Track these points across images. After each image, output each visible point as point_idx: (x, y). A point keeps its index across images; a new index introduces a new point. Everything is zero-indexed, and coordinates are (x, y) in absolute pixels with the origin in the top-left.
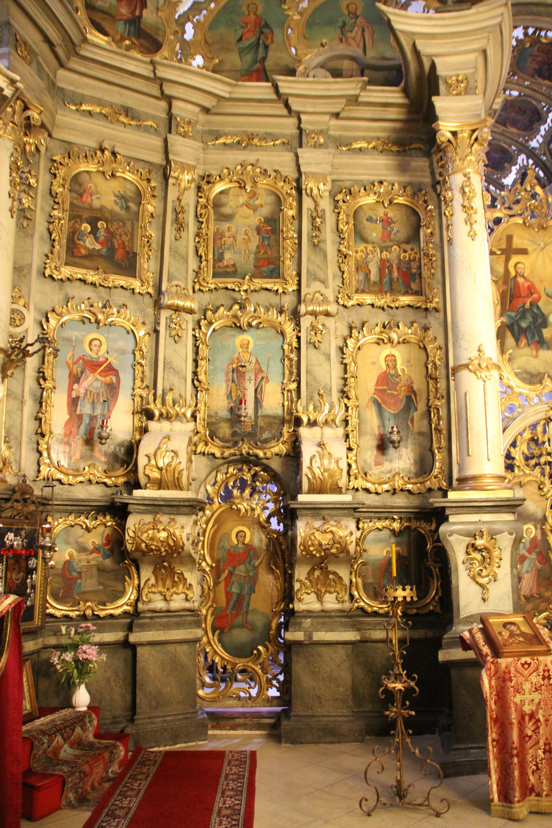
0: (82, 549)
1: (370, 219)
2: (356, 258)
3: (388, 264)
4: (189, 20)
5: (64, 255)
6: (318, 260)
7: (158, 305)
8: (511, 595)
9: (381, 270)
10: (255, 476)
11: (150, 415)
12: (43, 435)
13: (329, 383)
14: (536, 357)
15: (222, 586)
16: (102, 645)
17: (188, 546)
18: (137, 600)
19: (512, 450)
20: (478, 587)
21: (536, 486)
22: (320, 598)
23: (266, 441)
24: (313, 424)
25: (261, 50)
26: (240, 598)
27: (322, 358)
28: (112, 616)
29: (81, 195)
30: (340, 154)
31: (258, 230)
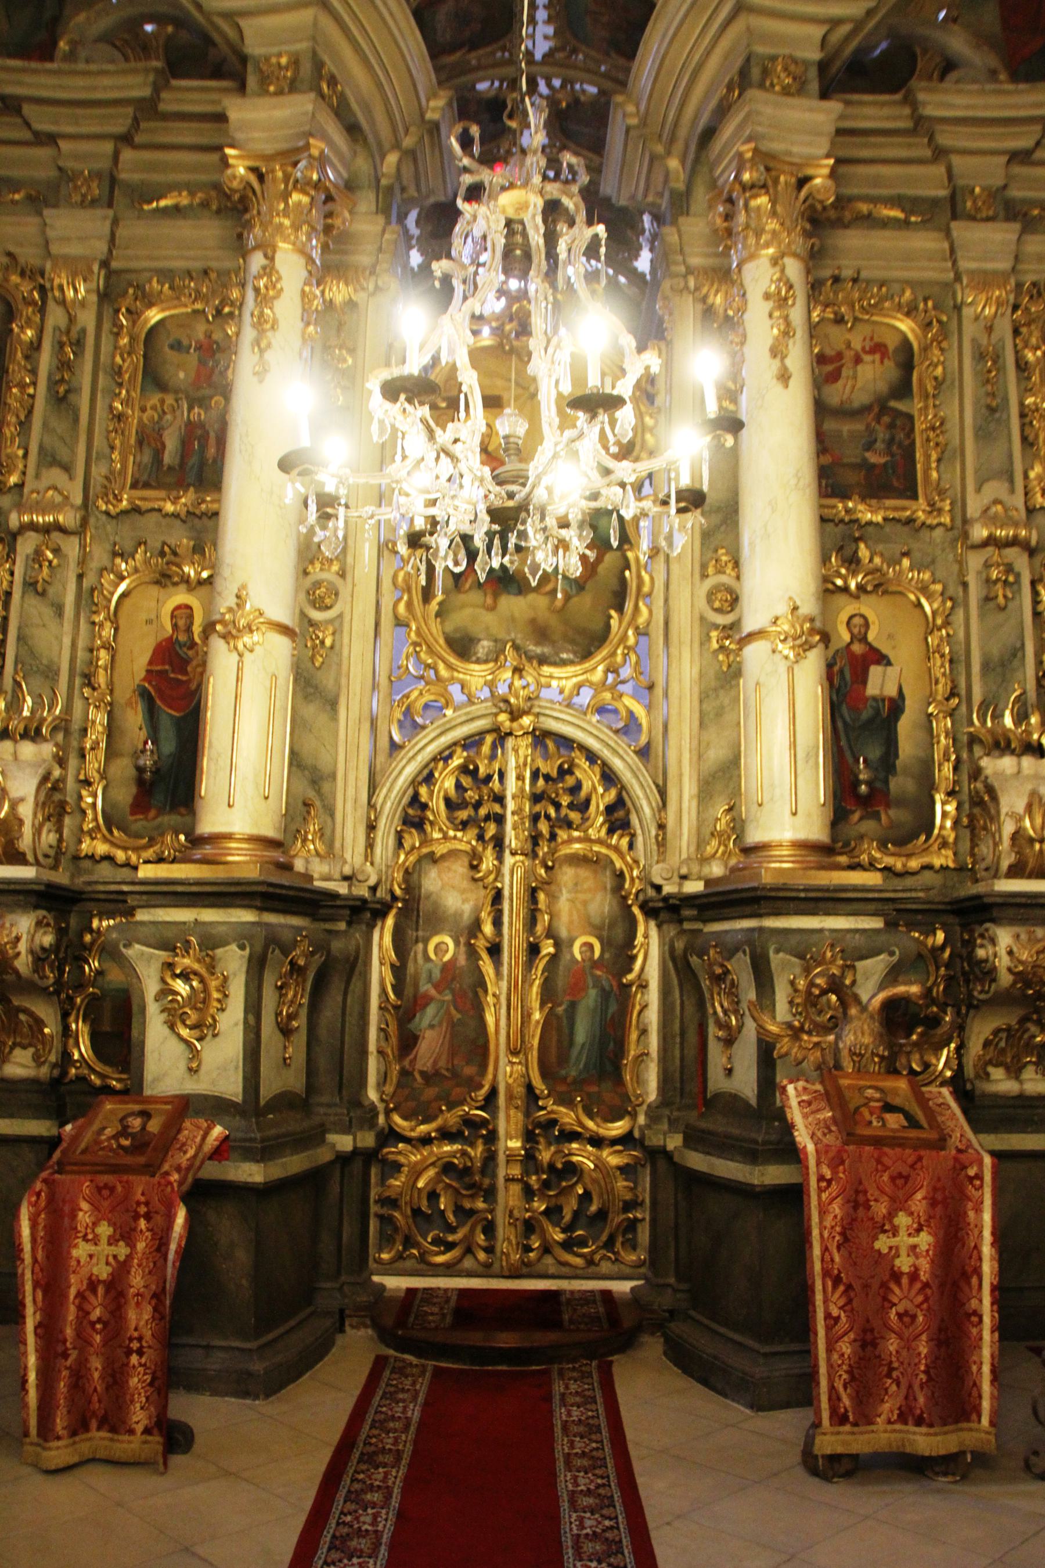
1: (177, 346)
2: (140, 420)
3: (199, 432)
6: (61, 426)
8: (241, 1064)
9: (185, 444)
13: (56, 659)
14: (492, 608)
19: (423, 790)
20: (182, 1046)
21: (466, 861)
27: (48, 612)
30: (139, 218)
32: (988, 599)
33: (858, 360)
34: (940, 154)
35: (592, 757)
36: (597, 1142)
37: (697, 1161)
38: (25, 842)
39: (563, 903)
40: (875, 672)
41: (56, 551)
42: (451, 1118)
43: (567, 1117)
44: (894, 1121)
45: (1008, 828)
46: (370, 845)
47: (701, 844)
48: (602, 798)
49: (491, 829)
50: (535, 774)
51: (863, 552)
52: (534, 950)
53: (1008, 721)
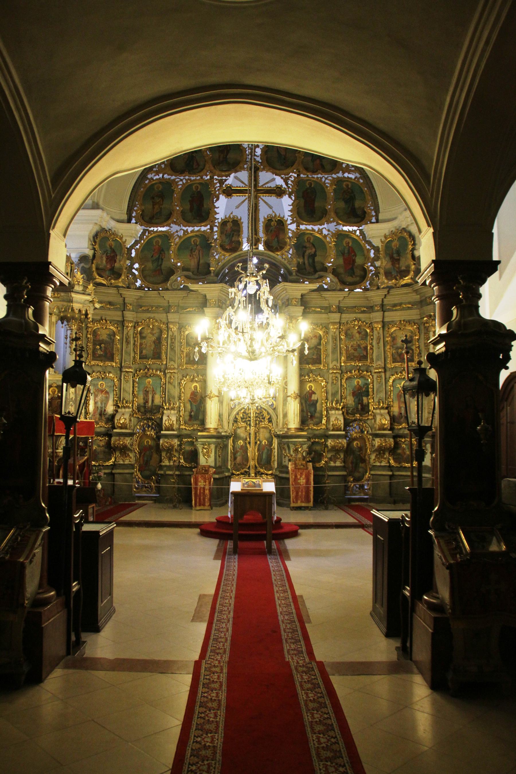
0: (99, 446)
4: (133, 248)
5: (91, 358)
7: (121, 371)
10: (153, 424)
11: (119, 407)
12: (87, 414)
15: (141, 458)
16: (105, 473)
17: (129, 446)
18: (115, 460)
22: (169, 462)
23: (155, 413)
24: (168, 409)
25: (160, 260)
26: (147, 461)
27: (173, 387)
28: (107, 465)
29: (96, 336)
31: (154, 342)
32: (333, 383)
33: (312, 339)
34: (326, 300)
35: (265, 410)
36: (267, 474)
37: (281, 475)
38: (174, 428)
39: (261, 435)
40: (313, 395)
41: (174, 376)
42: (243, 471)
43: (262, 470)
44: (302, 467)
45: (331, 423)
46: (228, 426)
47: (283, 425)
48: (267, 417)
49: (249, 423)
50: (256, 413)
51: (311, 375)
52: (256, 443)
53: (334, 405)
